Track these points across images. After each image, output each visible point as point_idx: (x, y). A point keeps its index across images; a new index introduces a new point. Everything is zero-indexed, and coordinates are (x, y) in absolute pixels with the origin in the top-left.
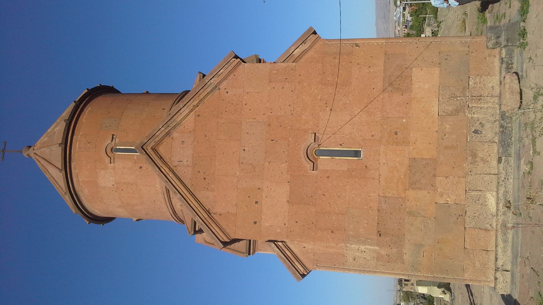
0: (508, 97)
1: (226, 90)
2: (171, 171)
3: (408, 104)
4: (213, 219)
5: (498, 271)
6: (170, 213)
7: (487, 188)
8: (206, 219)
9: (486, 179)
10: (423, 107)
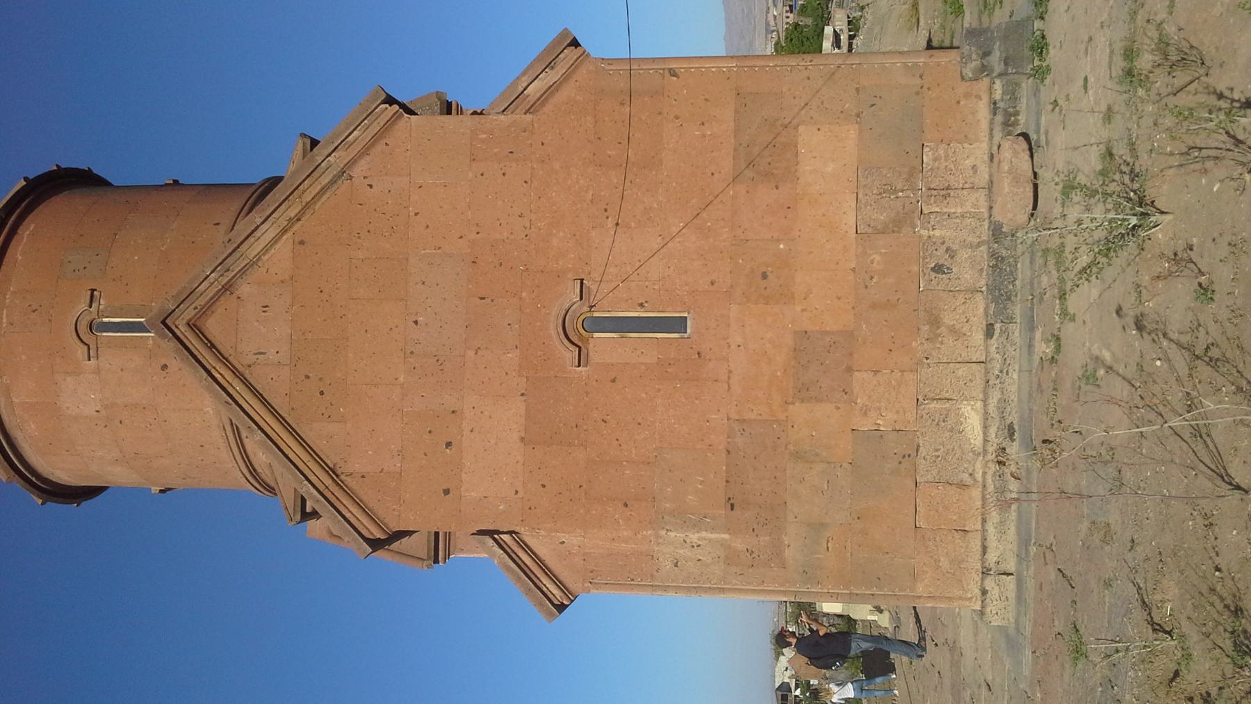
0: (1006, 190)
1: (368, 181)
2: (238, 377)
3: (789, 208)
4: (344, 487)
5: (988, 574)
6: (241, 470)
7: (963, 394)
8: (327, 487)
9: (960, 373)
10: (824, 215)
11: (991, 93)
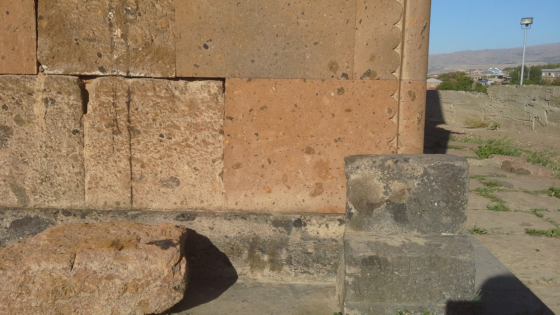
0: (34, 267)
11: (323, 215)
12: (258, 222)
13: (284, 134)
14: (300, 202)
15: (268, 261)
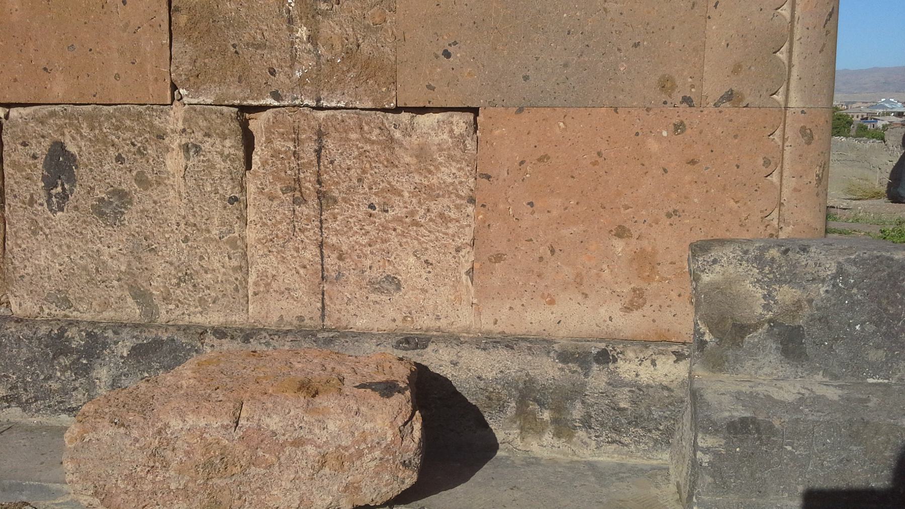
0: (176, 424)
11: (645, 344)
12: (533, 354)
13: (577, 203)
14: (605, 321)
15: (550, 421)
